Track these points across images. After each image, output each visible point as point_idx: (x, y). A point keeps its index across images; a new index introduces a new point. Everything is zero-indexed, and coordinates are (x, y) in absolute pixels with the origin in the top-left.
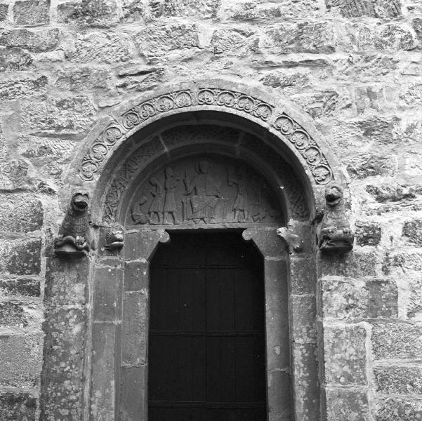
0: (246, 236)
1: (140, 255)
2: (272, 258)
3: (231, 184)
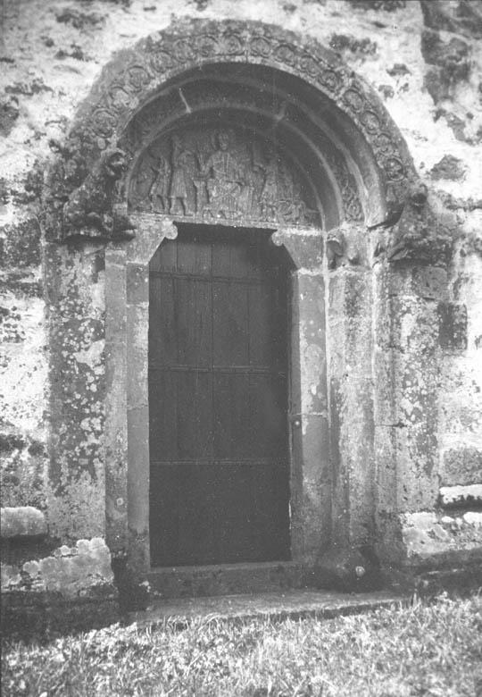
0: (276, 239)
1: (143, 257)
2: (309, 272)
3: (256, 169)
